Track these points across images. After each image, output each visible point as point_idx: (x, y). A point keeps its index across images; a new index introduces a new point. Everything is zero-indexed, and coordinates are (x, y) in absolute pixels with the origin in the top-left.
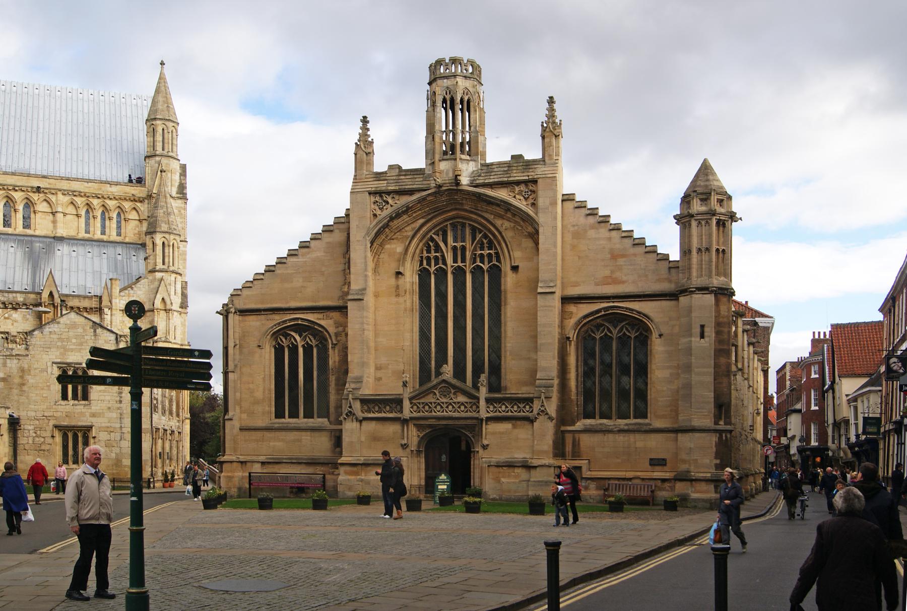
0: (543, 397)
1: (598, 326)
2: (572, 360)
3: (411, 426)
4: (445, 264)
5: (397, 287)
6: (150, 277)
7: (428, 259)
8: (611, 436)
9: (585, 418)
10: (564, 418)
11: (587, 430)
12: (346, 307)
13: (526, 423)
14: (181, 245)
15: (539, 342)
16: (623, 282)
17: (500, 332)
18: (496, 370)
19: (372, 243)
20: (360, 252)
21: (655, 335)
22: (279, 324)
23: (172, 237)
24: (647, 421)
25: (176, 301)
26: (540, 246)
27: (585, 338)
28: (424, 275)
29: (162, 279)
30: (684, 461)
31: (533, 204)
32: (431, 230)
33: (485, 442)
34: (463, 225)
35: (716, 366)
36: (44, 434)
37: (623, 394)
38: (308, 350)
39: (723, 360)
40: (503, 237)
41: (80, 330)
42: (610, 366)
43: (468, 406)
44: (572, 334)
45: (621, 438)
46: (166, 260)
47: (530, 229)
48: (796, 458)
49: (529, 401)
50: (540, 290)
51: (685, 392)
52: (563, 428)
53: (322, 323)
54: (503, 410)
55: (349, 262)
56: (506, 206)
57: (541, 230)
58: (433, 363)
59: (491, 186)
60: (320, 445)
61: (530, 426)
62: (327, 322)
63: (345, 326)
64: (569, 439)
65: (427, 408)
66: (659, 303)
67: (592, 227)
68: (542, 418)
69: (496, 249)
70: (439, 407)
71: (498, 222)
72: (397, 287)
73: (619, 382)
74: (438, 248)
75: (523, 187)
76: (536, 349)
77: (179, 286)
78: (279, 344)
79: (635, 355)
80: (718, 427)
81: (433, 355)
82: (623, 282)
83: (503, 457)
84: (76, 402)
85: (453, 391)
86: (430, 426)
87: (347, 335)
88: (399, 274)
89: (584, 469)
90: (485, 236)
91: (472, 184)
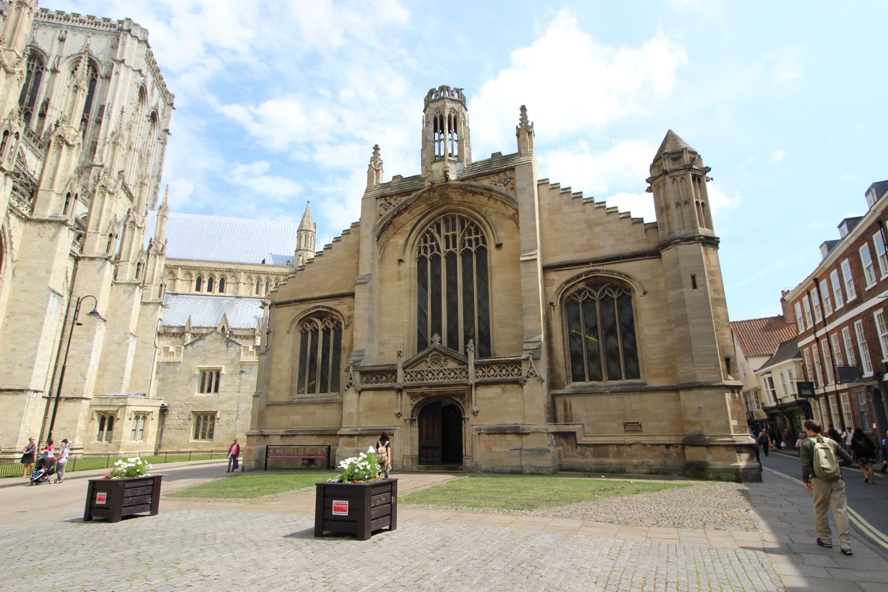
0: (531, 359)
3: (404, 393)
5: (399, 273)
7: (425, 248)
8: (604, 399)
9: (574, 380)
13: (516, 386)
15: (524, 306)
16: (601, 247)
17: (488, 304)
19: (378, 237)
22: (304, 312)
24: (639, 381)
27: (567, 305)
28: (421, 261)
30: (693, 423)
31: (512, 188)
32: (427, 224)
33: (475, 409)
34: (454, 219)
38: (326, 332)
43: (458, 372)
45: (614, 400)
47: (511, 211)
49: (517, 363)
50: (522, 259)
54: (492, 374)
57: (520, 208)
62: (341, 307)
65: (419, 376)
66: (639, 262)
67: (566, 203)
68: (531, 380)
69: (482, 233)
70: (430, 375)
72: (399, 273)
74: (433, 239)
81: (429, 329)
82: (601, 247)
83: (494, 423)
85: (443, 358)
86: (423, 394)
88: (400, 261)
89: (578, 435)
90: (472, 224)
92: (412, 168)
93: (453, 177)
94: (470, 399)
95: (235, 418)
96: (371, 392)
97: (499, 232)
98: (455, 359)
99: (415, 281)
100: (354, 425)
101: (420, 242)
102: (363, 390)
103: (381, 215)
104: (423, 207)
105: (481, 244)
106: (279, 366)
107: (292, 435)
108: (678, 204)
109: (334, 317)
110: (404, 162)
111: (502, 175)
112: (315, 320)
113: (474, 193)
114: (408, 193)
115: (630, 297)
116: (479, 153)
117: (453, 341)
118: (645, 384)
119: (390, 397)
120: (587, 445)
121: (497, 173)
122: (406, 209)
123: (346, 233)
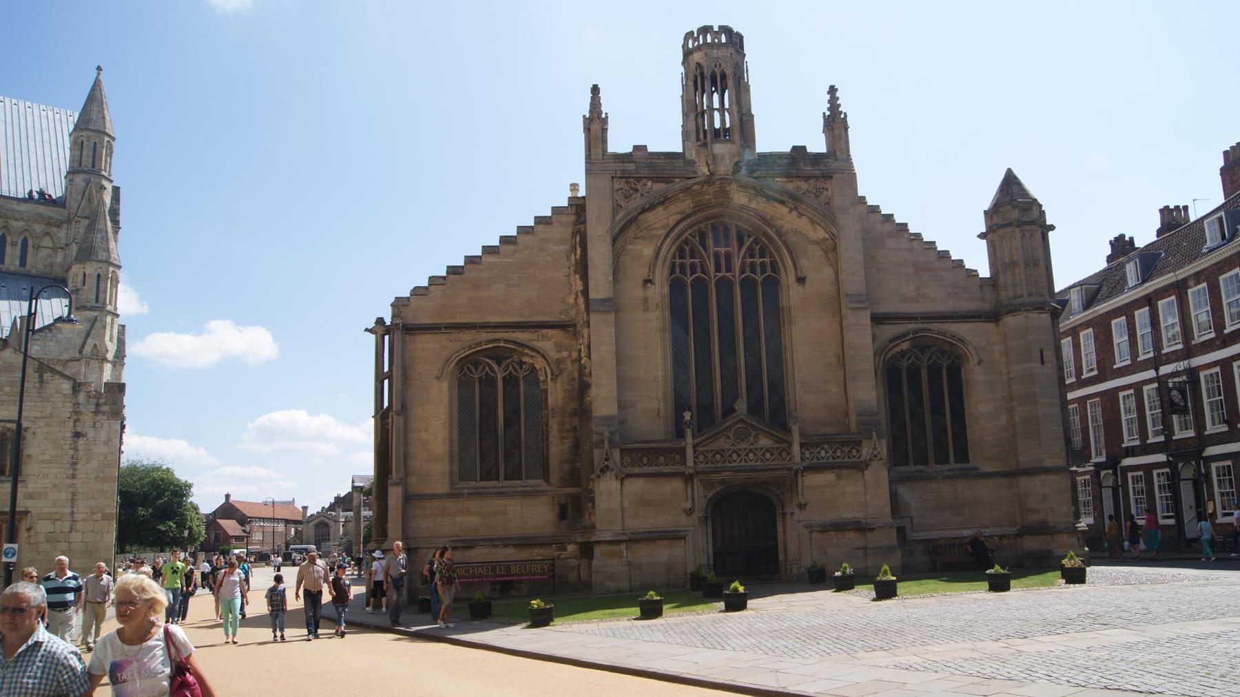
4: (709, 276)
7: (682, 267)
19: (614, 240)
20: (600, 255)
21: (973, 362)
28: (676, 287)
29: (96, 320)
32: (686, 230)
40: (785, 243)
47: (821, 234)
53: (538, 345)
60: (532, 513)
67: (890, 235)
68: (874, 464)
69: (772, 256)
70: (735, 456)
72: (646, 299)
83: (829, 517)
85: (753, 434)
86: (722, 482)
88: (648, 281)
92: (666, 136)
93: (744, 171)
95: (68, 529)
96: (642, 480)
100: (617, 527)
101: (674, 254)
102: (628, 476)
104: (686, 205)
105: (769, 272)
106: (424, 435)
107: (469, 544)
108: (1027, 265)
109: (526, 359)
111: (812, 181)
118: (977, 469)
120: (917, 541)
121: (807, 178)
123: (540, 220)
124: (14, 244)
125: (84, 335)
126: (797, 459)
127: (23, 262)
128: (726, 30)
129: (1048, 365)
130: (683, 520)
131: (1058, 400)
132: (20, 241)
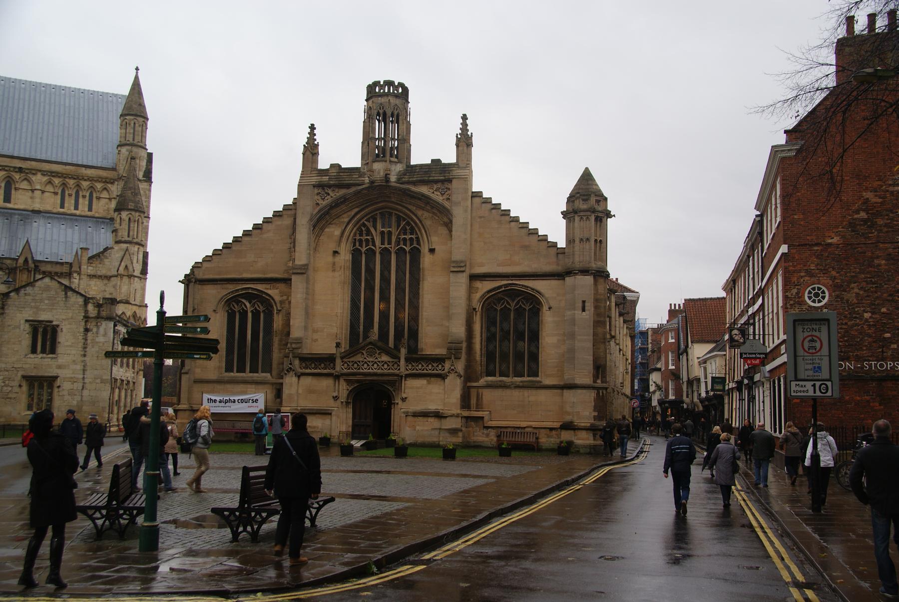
1: (500, 300)
2: (477, 327)
3: (342, 380)
4: (375, 246)
5: (334, 264)
6: (116, 247)
7: (361, 241)
8: (508, 392)
10: (469, 376)
11: (489, 386)
12: (290, 280)
13: (439, 379)
14: (145, 220)
17: (418, 302)
18: (414, 334)
19: (314, 227)
20: (303, 235)
21: (545, 308)
23: (137, 214)
24: (538, 379)
25: (138, 268)
26: (453, 233)
28: (356, 254)
29: (127, 250)
30: (569, 414)
31: (448, 199)
33: (404, 396)
34: (390, 214)
35: (595, 334)
36: (12, 384)
37: (519, 356)
38: (256, 314)
39: (600, 330)
41: (53, 293)
42: (508, 332)
44: (478, 307)
45: (516, 393)
46: (131, 233)
47: (446, 220)
48: (658, 409)
49: (440, 360)
51: (570, 356)
52: (469, 384)
53: (269, 292)
54: (419, 368)
55: (294, 242)
56: (426, 201)
57: (454, 221)
58: (361, 327)
59: (414, 183)
61: (442, 382)
62: (274, 292)
63: (289, 295)
64: (473, 392)
65: (356, 365)
66: (549, 282)
70: (366, 365)
71: (419, 213)
72: (334, 264)
73: (515, 346)
74: (369, 233)
75: (439, 185)
76: (449, 317)
77: (141, 256)
78: (231, 309)
79: (529, 324)
80: (596, 385)
83: (419, 408)
84: (44, 355)
86: (357, 381)
87: (290, 303)
88: (336, 253)
89: (486, 419)
90: (408, 224)
91: (399, 181)
92: (352, 159)
93: (393, 178)
94: (399, 389)
97: (435, 238)
98: (388, 353)
99: (349, 273)
101: (355, 235)
103: (318, 204)
110: (344, 149)
112: (244, 301)
113: (413, 197)
114: (348, 186)
115: (539, 310)
116: (420, 156)
117: (383, 334)
119: (327, 383)
121: (436, 182)
122: (344, 201)
123: (277, 214)
124: (84, 197)
125: (120, 259)
126: (403, 369)
127: (90, 209)
128: (389, 83)
129: (587, 312)
130: (332, 403)
131: (591, 338)
132: (88, 195)
